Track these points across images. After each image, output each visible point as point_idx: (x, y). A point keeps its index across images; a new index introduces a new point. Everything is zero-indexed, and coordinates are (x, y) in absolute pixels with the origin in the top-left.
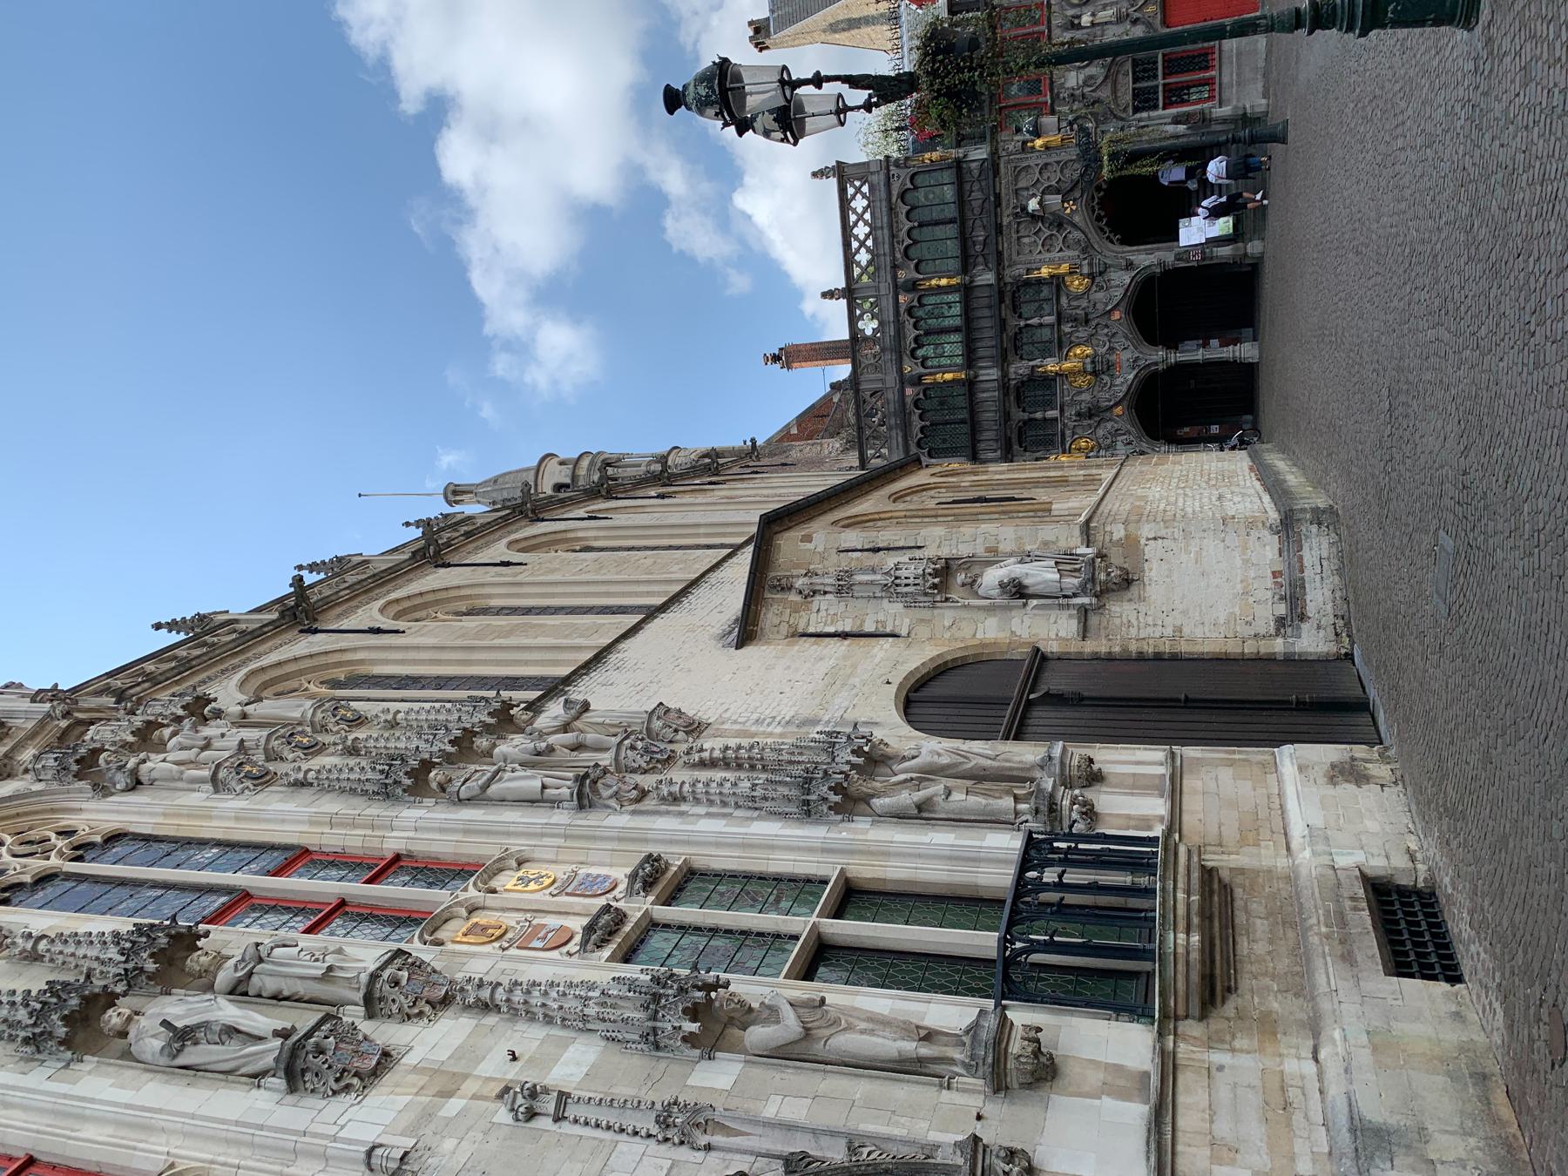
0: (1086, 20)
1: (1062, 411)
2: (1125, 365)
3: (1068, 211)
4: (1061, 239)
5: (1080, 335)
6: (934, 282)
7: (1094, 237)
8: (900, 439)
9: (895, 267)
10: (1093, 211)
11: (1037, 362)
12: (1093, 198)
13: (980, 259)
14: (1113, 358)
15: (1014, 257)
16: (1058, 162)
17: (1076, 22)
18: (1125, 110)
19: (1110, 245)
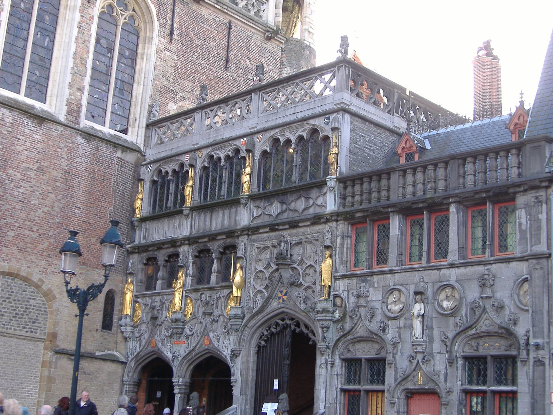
0: (418, 308)
1: (159, 294)
2: (176, 348)
3: (280, 295)
4: (261, 289)
5: (200, 308)
6: (248, 170)
7: (260, 319)
8: (164, 155)
9: (265, 130)
10: (283, 320)
11: (190, 270)
12: (292, 319)
13: (260, 213)
14: (183, 338)
15: (256, 244)
16: (315, 283)
17: (418, 297)
18: (349, 351)
19: (257, 336)
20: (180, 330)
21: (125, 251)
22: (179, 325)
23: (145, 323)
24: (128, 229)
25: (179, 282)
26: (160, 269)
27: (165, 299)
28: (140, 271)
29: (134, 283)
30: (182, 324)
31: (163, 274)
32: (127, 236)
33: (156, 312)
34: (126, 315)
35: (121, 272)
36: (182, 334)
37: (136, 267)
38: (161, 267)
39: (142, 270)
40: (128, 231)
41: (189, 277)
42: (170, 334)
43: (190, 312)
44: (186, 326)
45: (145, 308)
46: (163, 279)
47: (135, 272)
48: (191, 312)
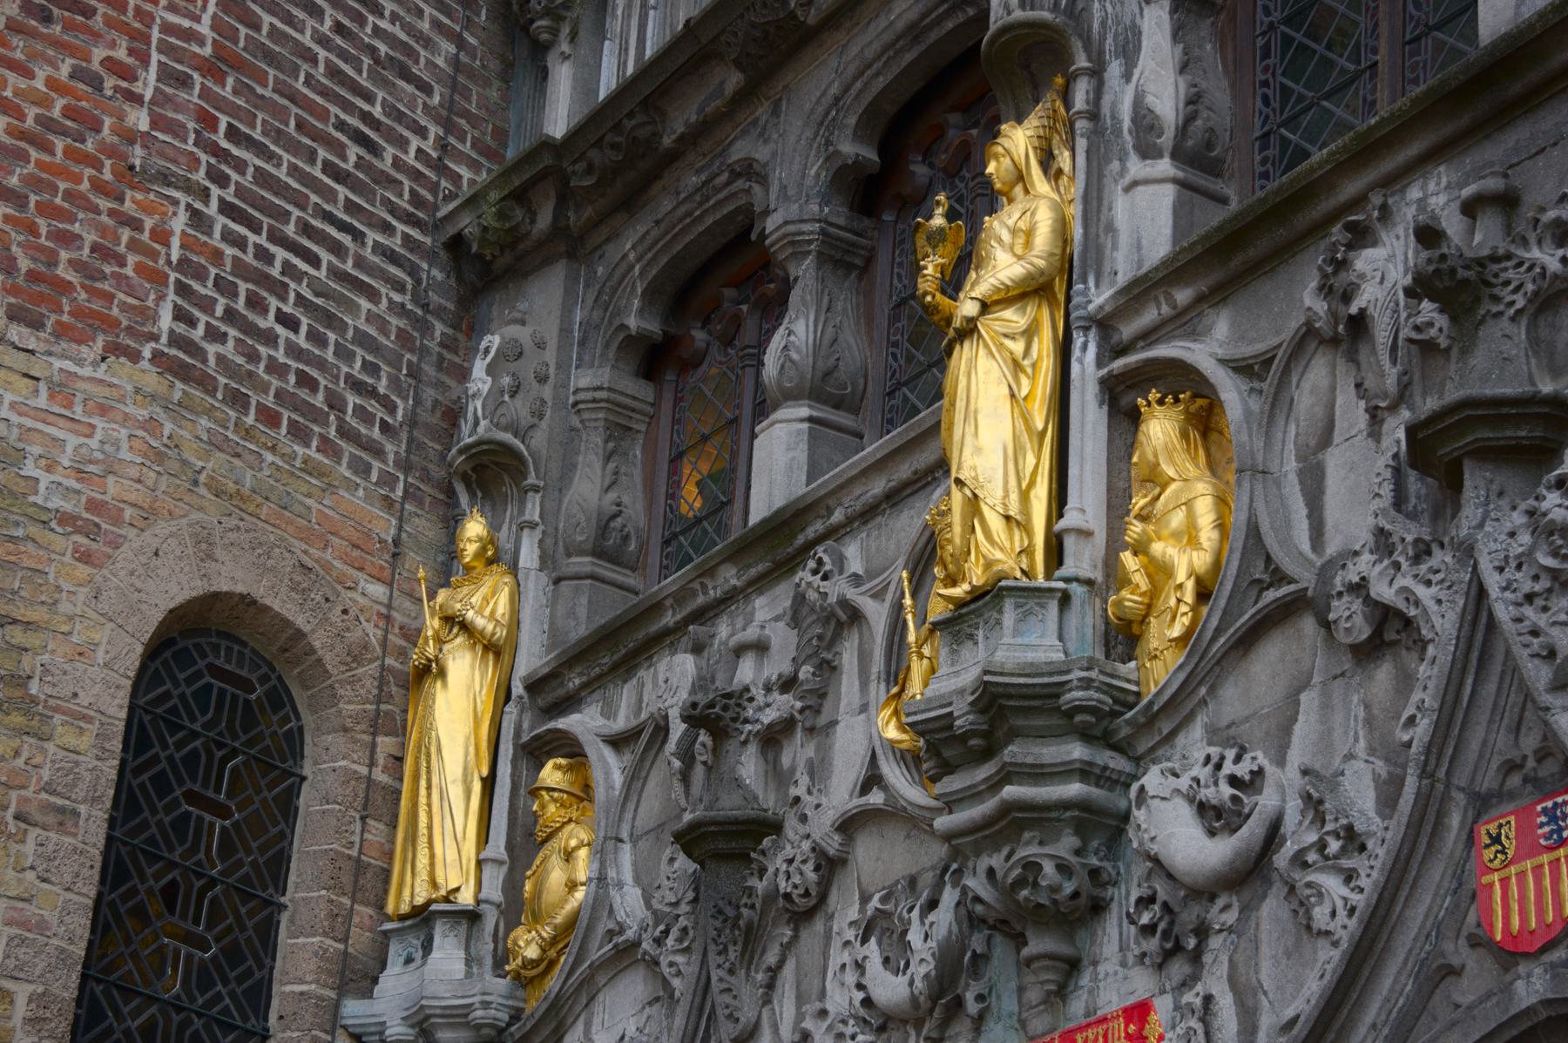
20: (1066, 845)
21: (430, 256)
22: (1038, 774)
23: (625, 955)
24: (460, 43)
25: (1000, 226)
26: (795, 297)
27: (855, 565)
28: (594, 441)
29: (529, 555)
30: (1077, 751)
31: (825, 346)
32: (449, 105)
33: (749, 766)
34: (422, 918)
35: (379, 453)
36: (1098, 908)
37: (547, 392)
38: (805, 272)
39: (618, 431)
40: (455, 62)
41: (1137, 167)
42: (923, 965)
43: (1187, 563)
44: (1152, 779)
45: (635, 778)
46: (816, 394)
47: (539, 439)
48: (1201, 560)
